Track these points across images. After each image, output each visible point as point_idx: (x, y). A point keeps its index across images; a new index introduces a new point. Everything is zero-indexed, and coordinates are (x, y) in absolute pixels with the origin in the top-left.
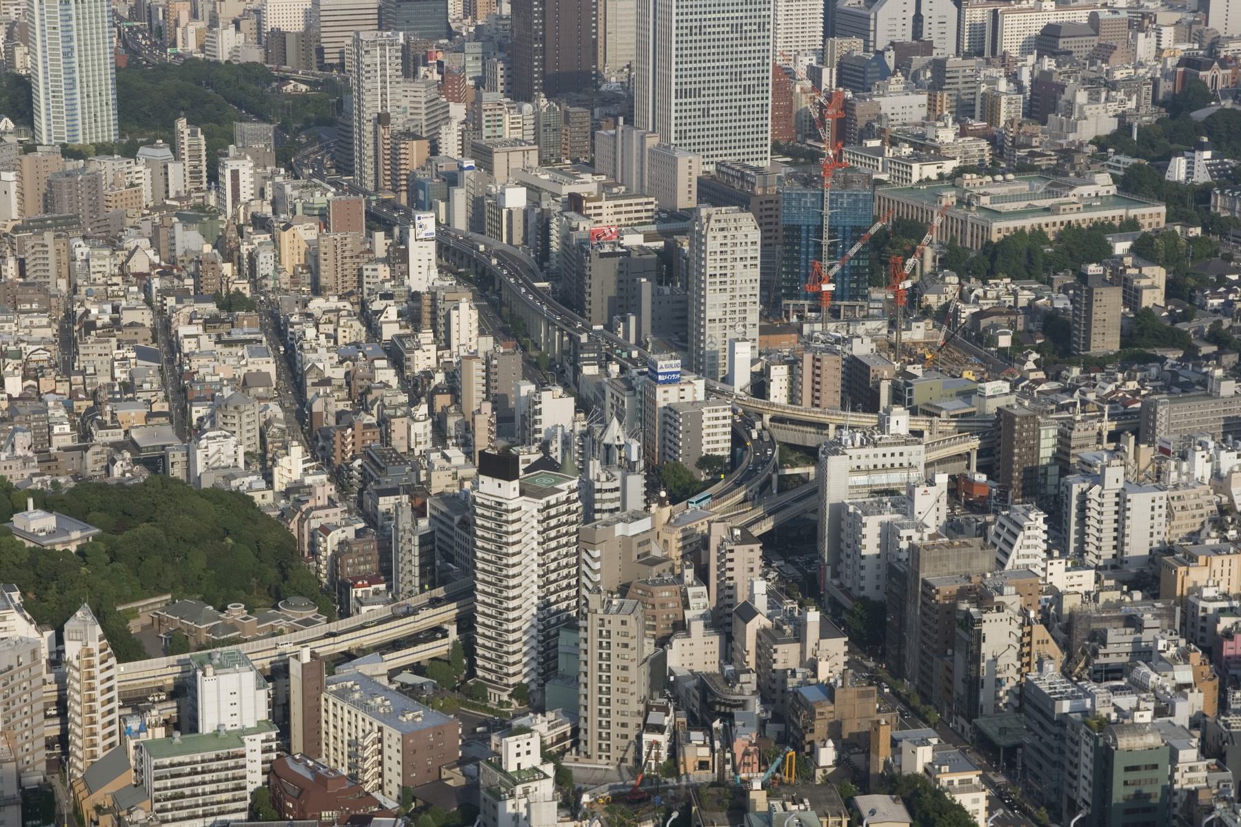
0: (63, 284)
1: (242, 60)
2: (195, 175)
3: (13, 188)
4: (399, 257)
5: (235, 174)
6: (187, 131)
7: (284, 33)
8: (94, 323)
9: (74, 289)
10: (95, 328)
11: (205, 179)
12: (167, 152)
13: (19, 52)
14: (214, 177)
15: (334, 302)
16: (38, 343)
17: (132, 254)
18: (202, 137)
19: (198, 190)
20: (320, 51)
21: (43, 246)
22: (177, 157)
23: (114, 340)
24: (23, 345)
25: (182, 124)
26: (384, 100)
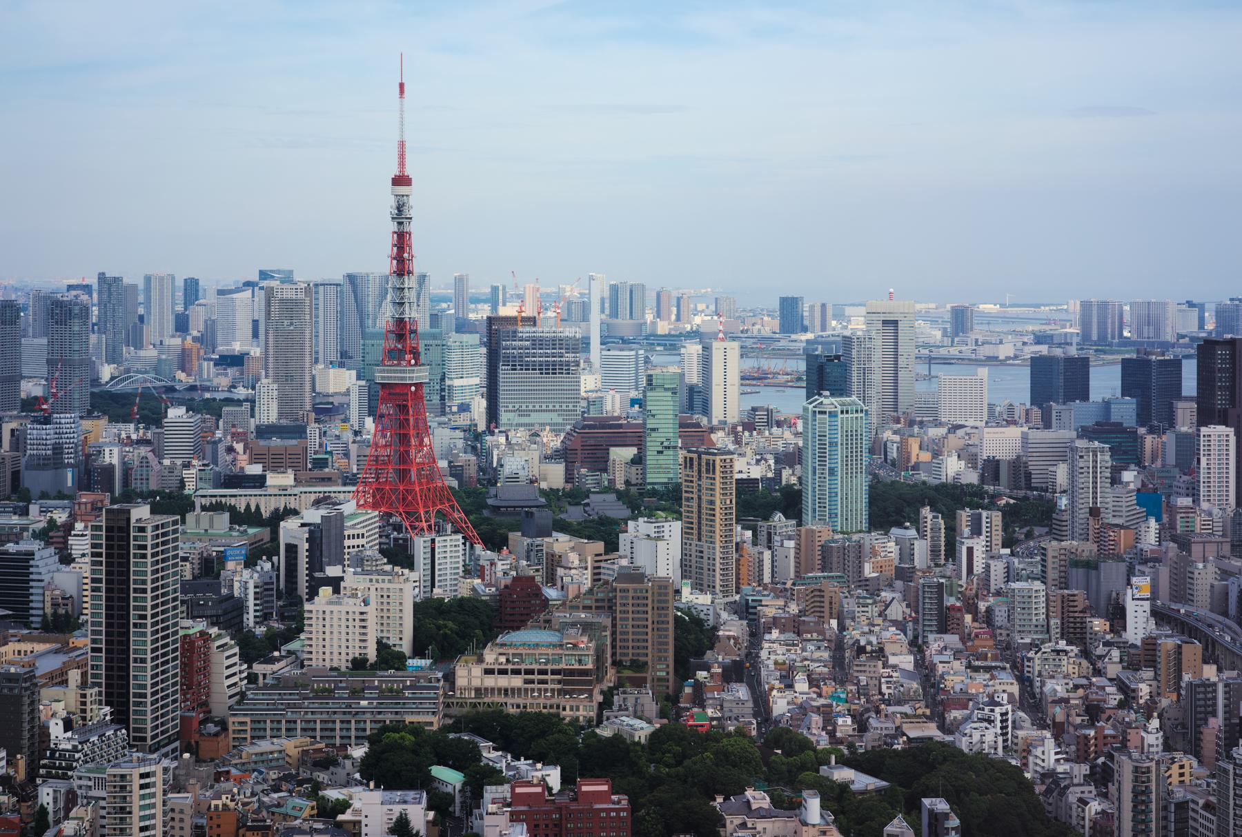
0: (834, 623)
1: (964, 481)
2: (935, 551)
3: (792, 552)
4: (1117, 616)
5: (970, 551)
6: (930, 516)
7: (998, 461)
8: (864, 647)
9: (842, 627)
10: (866, 653)
11: (943, 557)
12: (912, 533)
13: (786, 473)
14: (951, 552)
15: (1062, 644)
16: (820, 661)
17: (887, 606)
18: (942, 522)
19: (937, 565)
20: (1028, 476)
21: (820, 591)
22: (923, 537)
23: (880, 663)
24: (806, 663)
25: (926, 512)
26: (1095, 498)
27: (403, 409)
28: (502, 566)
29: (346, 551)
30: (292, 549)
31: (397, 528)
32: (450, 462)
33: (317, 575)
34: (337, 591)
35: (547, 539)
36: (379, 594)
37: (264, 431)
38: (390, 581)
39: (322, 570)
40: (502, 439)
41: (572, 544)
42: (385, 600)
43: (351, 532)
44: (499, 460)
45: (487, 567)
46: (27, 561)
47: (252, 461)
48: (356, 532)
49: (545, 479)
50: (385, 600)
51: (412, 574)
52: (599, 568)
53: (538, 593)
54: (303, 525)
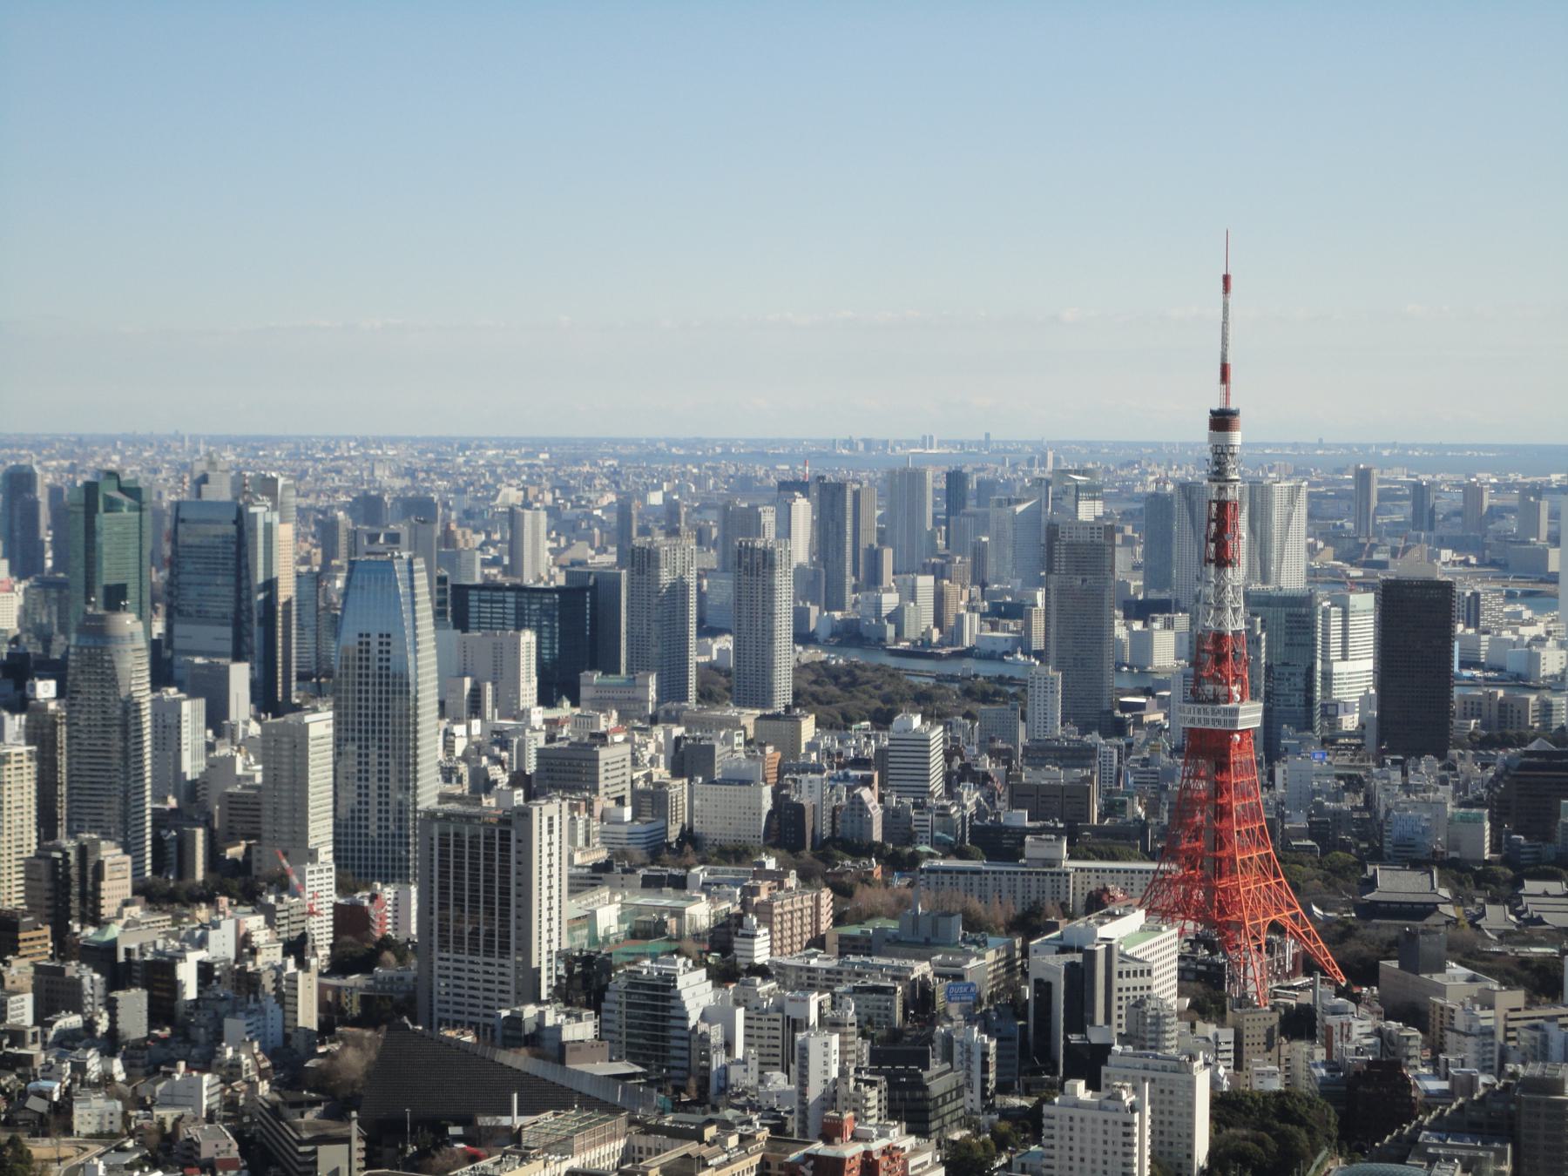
27: (1222, 765)
28: (1359, 1029)
29: (1124, 994)
30: (1044, 988)
31: (1212, 947)
32: (1310, 816)
33: (1075, 1038)
34: (1093, 1085)
35: (1437, 978)
36: (1158, 1086)
37: (1040, 753)
38: (1175, 1071)
39: (1082, 1030)
40: (1396, 775)
41: (1474, 989)
42: (1166, 1097)
43: (1132, 966)
44: (1388, 811)
45: (1337, 1030)
46: (668, 988)
47: (1015, 803)
48: (1139, 967)
49: (1457, 849)
50: (1166, 1097)
51: (1221, 1032)
52: (1514, 1029)
53: (1405, 1084)
54: (1063, 950)
